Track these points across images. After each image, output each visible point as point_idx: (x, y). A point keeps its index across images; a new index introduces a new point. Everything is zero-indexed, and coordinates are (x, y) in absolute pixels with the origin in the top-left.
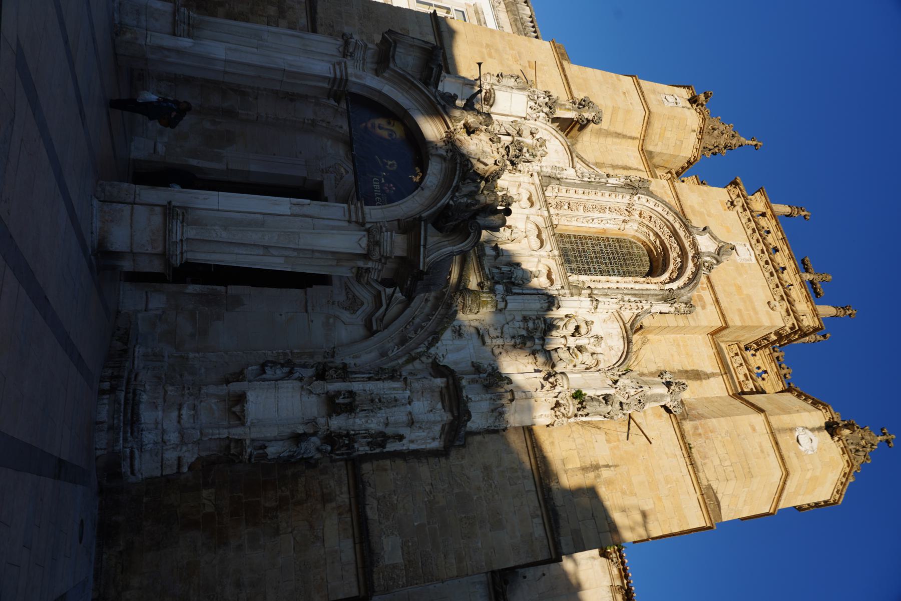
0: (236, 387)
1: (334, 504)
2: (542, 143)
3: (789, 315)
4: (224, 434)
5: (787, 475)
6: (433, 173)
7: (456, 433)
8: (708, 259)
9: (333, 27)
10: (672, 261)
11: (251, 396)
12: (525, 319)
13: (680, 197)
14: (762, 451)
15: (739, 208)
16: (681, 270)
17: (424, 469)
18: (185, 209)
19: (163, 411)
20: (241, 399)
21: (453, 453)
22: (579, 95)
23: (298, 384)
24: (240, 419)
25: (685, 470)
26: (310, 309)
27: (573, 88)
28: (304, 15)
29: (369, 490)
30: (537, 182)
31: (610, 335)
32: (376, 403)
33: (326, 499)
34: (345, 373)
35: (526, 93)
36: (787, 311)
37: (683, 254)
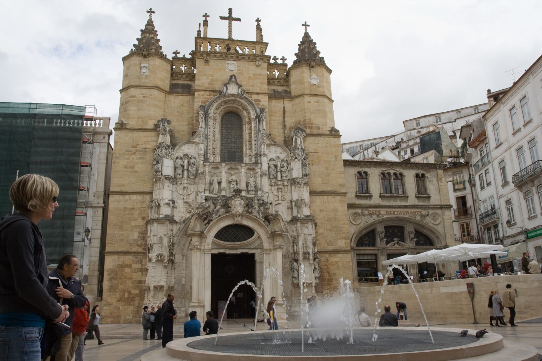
2: (186, 155)
4: (314, 288)
5: (326, 96)
7: (309, 219)
8: (240, 90)
10: (237, 106)
12: (271, 186)
14: (318, 102)
15: (208, 58)
17: (321, 231)
21: (316, 221)
22: (151, 124)
24: (311, 284)
25: (323, 139)
27: (146, 127)
28: (127, 257)
29: (326, 248)
30: (208, 164)
31: (276, 151)
32: (305, 245)
33: (327, 260)
34: (296, 253)
35: (164, 158)
36: (261, 59)
37: (235, 101)
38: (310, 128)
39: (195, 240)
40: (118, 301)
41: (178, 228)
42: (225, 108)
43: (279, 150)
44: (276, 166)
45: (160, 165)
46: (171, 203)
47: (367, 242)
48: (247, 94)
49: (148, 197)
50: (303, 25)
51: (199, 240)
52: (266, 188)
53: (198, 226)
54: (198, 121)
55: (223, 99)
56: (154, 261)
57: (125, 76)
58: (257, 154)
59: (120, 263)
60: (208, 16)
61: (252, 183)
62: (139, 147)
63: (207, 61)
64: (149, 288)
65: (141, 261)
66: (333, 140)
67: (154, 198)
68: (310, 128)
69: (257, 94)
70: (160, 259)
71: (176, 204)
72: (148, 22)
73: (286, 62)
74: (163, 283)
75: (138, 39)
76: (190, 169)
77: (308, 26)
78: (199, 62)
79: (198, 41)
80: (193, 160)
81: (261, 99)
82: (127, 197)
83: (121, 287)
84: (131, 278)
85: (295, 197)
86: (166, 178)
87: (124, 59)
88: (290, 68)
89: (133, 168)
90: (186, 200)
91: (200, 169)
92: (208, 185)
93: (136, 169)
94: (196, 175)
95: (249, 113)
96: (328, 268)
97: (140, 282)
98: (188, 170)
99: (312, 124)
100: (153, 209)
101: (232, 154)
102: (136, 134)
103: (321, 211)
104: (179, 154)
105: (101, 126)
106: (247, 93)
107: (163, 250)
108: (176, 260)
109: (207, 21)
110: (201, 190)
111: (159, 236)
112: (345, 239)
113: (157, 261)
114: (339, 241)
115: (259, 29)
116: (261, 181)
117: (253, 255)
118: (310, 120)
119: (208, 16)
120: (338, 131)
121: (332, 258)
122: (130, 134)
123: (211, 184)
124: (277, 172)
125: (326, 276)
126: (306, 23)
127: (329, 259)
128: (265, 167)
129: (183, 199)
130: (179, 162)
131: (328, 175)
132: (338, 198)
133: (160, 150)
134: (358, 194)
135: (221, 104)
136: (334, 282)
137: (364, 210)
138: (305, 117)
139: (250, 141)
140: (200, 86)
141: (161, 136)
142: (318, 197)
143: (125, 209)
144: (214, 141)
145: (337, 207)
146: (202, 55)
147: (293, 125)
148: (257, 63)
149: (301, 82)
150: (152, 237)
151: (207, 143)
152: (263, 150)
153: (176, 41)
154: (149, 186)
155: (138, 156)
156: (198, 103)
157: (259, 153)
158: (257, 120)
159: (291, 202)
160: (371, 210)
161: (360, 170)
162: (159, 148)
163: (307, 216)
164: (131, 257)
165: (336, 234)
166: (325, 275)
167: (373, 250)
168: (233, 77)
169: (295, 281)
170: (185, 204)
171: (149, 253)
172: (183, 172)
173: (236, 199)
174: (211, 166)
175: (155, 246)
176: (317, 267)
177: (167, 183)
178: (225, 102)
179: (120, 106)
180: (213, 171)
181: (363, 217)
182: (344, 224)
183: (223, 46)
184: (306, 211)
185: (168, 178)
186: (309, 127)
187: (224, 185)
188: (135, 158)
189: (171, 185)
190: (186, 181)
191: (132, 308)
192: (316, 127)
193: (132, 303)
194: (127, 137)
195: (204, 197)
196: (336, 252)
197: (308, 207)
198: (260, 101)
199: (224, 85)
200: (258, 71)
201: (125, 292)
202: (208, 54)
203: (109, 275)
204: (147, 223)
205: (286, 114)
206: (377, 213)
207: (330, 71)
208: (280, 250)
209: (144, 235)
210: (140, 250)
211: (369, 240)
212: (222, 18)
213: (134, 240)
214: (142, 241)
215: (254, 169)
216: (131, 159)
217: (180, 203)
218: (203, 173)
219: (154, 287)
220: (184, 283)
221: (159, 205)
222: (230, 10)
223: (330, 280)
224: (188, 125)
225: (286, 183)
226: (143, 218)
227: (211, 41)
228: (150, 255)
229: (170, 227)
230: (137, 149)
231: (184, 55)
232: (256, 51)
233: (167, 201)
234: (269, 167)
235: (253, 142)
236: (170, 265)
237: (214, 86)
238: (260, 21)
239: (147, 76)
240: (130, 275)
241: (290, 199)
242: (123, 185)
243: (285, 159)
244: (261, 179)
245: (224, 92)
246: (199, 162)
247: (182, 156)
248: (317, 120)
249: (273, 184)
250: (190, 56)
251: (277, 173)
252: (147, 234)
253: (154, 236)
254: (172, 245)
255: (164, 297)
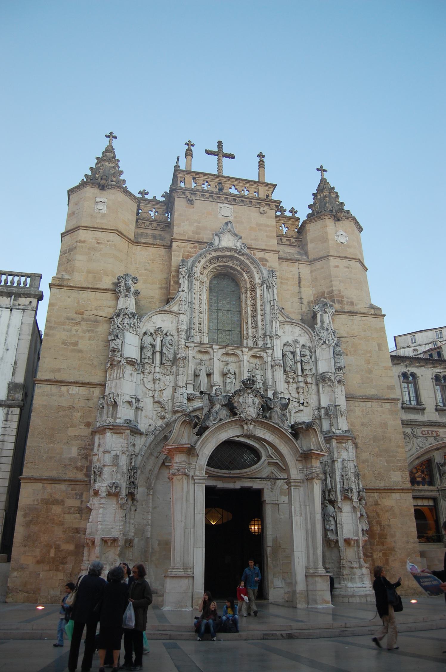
0: (341, 543)
1: (379, 500)
3: (269, 205)
4: (361, 548)
5: (359, 260)
6: (264, 434)
8: (238, 244)
9: (65, 465)
10: (234, 266)
11: (346, 536)
12: (288, 383)
13: (186, 239)
14: (348, 268)
15: (193, 197)
16: (242, 262)
18: (307, 568)
19: (354, 575)
20: (347, 542)
22: (107, 282)
23: (338, 514)
25: (359, 318)
26: (277, 502)
27: (98, 286)
30: (193, 345)
33: (377, 504)
36: (266, 204)
37: (232, 258)
38: (341, 302)
39: (179, 459)
40: (38, 562)
41: (142, 444)
42: (215, 268)
43: (297, 330)
44: (293, 353)
45: (119, 341)
46: (134, 401)
47: (419, 479)
48: (249, 250)
49: (97, 391)
50: (318, 169)
51: (186, 460)
52: (281, 387)
53: (186, 435)
54: (178, 283)
55: (214, 254)
56: (104, 495)
57: (71, 215)
58: (265, 335)
59: (46, 496)
60: (193, 145)
61: (258, 377)
62: (88, 314)
63: (190, 202)
64: (93, 542)
65: (81, 495)
66: (374, 321)
67: (107, 393)
68: (341, 302)
69: (263, 250)
70: (113, 493)
71: (141, 404)
72: (106, 148)
73: (296, 215)
74: (115, 534)
75: (91, 168)
76: (164, 351)
77: (326, 171)
78: (179, 204)
79: (179, 175)
80: (170, 337)
81: (268, 259)
82: (64, 389)
83: (44, 538)
84: (61, 524)
85: (325, 402)
86: (128, 363)
87: (71, 192)
88: (304, 223)
89: (76, 344)
90: (156, 399)
91: (180, 351)
92: (191, 377)
93: (80, 347)
94: (175, 360)
95: (252, 277)
96: (378, 515)
97: (77, 531)
98: (161, 353)
99: (343, 297)
100: (105, 411)
101: (231, 333)
102: (84, 294)
103: (362, 425)
104: (149, 328)
105: (28, 286)
106: (248, 248)
107: (119, 477)
108: (138, 497)
109: (192, 151)
110: (180, 384)
111: (113, 453)
112: (401, 469)
113: (109, 494)
114: (392, 472)
115: (261, 164)
116: (273, 375)
117: (259, 493)
118: (340, 291)
119: (193, 145)
120: (380, 309)
121: (384, 500)
122: (75, 294)
123: (196, 376)
124: (296, 363)
125: (377, 529)
126: (321, 167)
127: (380, 503)
128: (278, 355)
129: (153, 397)
130: (148, 340)
131: (370, 371)
132: (387, 406)
133: (120, 320)
134: (405, 405)
135: (210, 262)
136: (389, 540)
137: (415, 430)
138: (332, 286)
139: (254, 316)
140: (180, 234)
141: (122, 300)
142: (357, 403)
143: (60, 408)
144: (201, 313)
145: (389, 419)
146: (184, 193)
147: (312, 299)
148: (262, 209)
149: (324, 239)
150: (100, 453)
151: (191, 314)
152: (274, 330)
153: (147, 175)
154: (100, 373)
155: (85, 328)
156: (176, 260)
157: (268, 333)
158: (265, 286)
159: (319, 409)
160: (426, 429)
161: (405, 370)
162: (118, 315)
163: (346, 431)
164: (63, 487)
165: (387, 461)
166: (375, 528)
167: (432, 490)
168: (229, 225)
169: (331, 536)
170: (156, 405)
171: (95, 481)
172: (154, 354)
173: (246, 395)
174: (197, 349)
175: (106, 469)
176: (364, 514)
177: (129, 369)
178: (217, 258)
179: (61, 255)
180: (200, 356)
181: (415, 439)
182: (398, 446)
183: (213, 184)
184: (343, 425)
185: (131, 363)
186: (339, 302)
187: (217, 378)
188: (80, 330)
189: (135, 374)
190: (157, 369)
191: (60, 576)
192: (348, 302)
193: (61, 567)
194: (69, 298)
195: (186, 396)
196: (390, 490)
197: (344, 418)
198: (267, 261)
199: (216, 235)
200: (263, 220)
201: (51, 547)
202: (193, 192)
203: (25, 516)
204: (94, 433)
205: (302, 283)
206: (435, 435)
207: (360, 229)
208: (317, 481)
209: (87, 452)
210: (80, 476)
211: (423, 475)
212: (208, 152)
213: (71, 459)
214: (84, 460)
215: (260, 357)
216: (74, 332)
217: (147, 403)
218: (185, 358)
219: (102, 539)
220: (149, 535)
221: (115, 402)
222: (220, 143)
223: (383, 536)
224: (161, 288)
225: (309, 380)
226: (88, 425)
227: (196, 175)
228: (97, 486)
229: (132, 439)
230: (84, 316)
231: (155, 197)
232: (259, 195)
233: (128, 398)
234: (284, 355)
235: (259, 318)
236: (130, 502)
237: (201, 236)
238: (264, 157)
239: (103, 215)
240: (61, 519)
241: (317, 404)
242: (59, 370)
243: (308, 344)
244: (273, 372)
245: (216, 244)
246: (178, 341)
247: (153, 332)
248: (350, 292)
249: (291, 380)
250: (163, 199)
251: (294, 364)
252: (92, 450)
253: (105, 452)
254: (133, 470)
255: (117, 558)
